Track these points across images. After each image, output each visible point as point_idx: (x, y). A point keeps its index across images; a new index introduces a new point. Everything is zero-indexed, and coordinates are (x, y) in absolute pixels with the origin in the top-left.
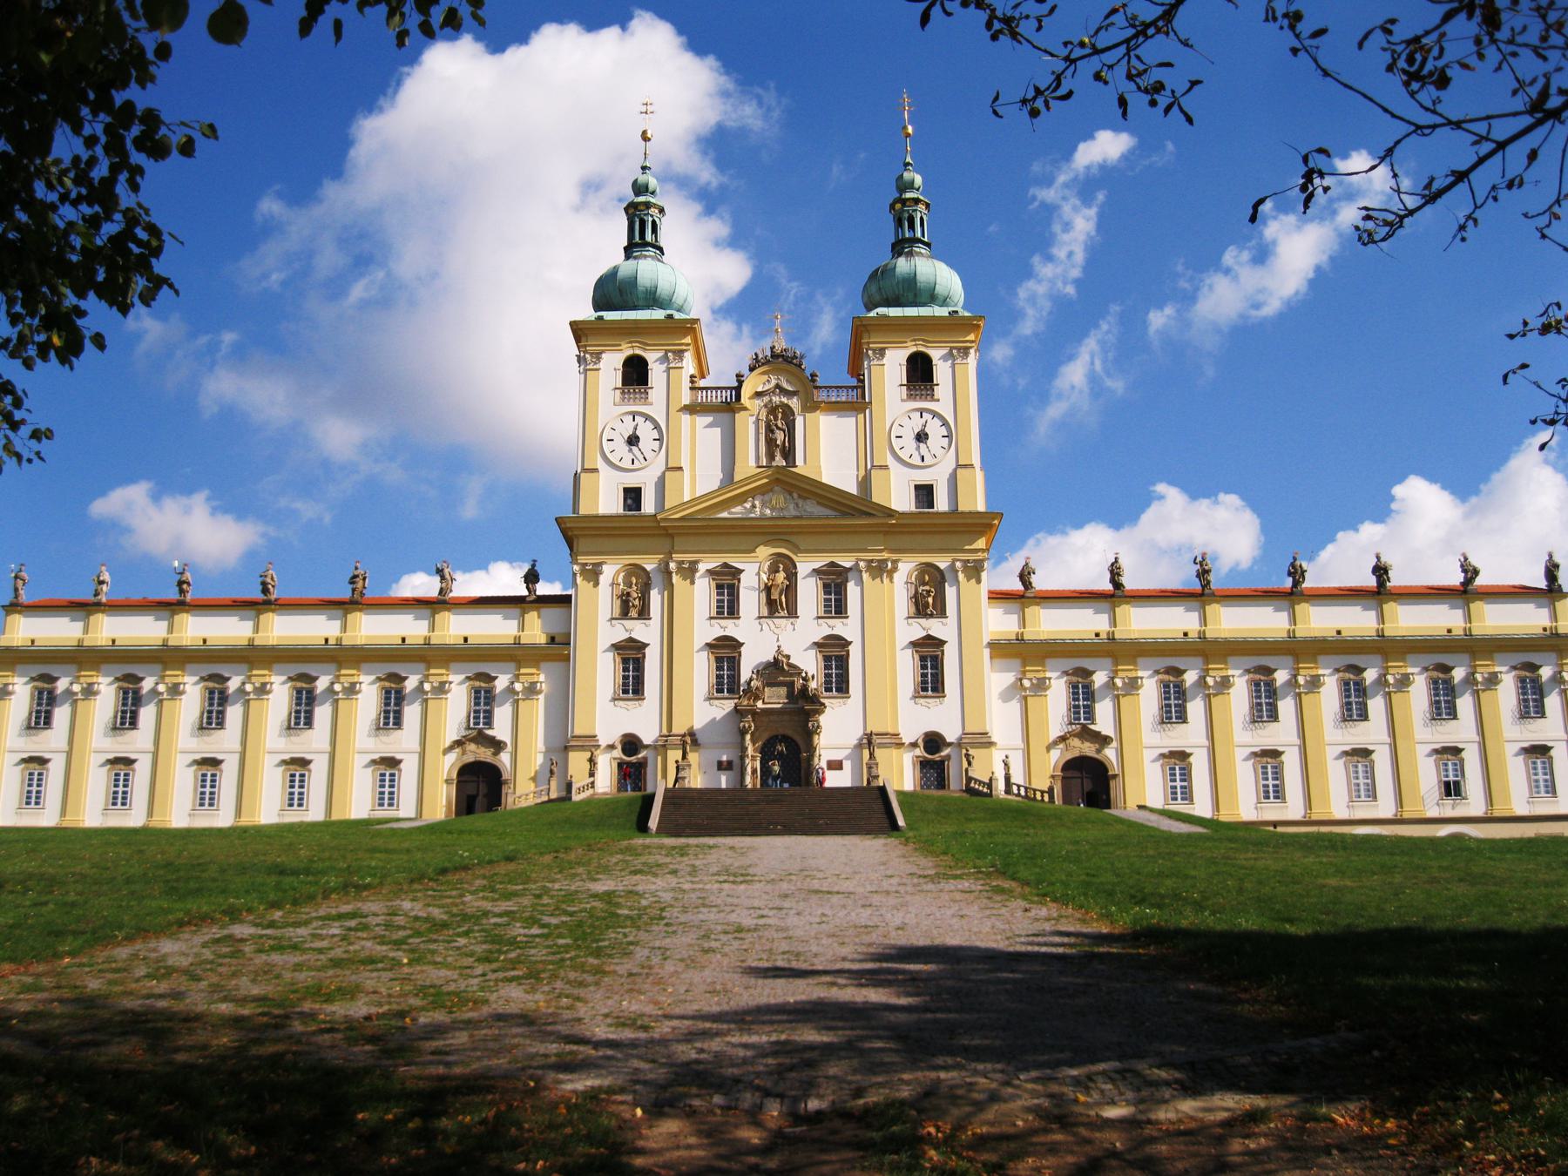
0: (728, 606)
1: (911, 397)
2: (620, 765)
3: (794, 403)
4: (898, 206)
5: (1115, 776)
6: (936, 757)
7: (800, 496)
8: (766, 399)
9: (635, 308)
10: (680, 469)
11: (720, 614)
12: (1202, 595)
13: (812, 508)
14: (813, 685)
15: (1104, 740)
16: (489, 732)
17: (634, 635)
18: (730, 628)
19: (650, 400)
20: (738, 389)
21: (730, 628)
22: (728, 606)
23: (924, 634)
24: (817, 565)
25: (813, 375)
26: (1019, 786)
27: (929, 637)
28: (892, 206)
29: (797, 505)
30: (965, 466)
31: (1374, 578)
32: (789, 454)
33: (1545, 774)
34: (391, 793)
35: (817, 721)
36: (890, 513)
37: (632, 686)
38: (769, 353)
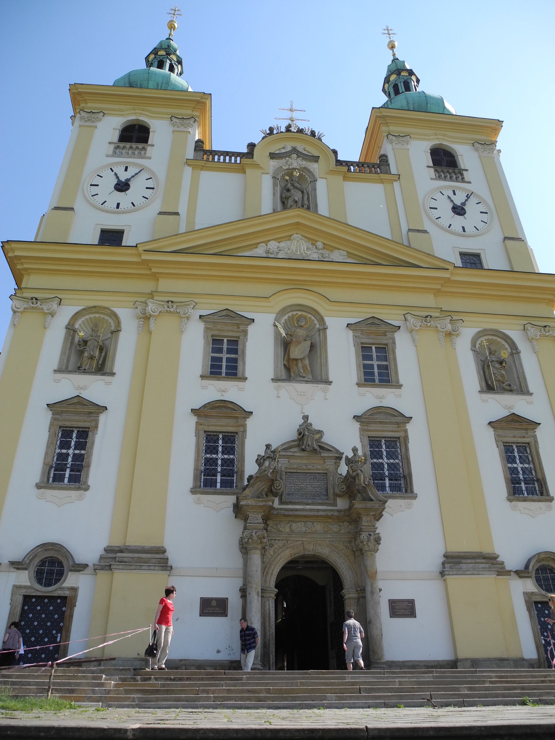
2: (27, 598)
3: (314, 167)
8: (282, 162)
10: (177, 214)
17: (86, 395)
19: (147, 155)
23: (505, 413)
24: (353, 321)
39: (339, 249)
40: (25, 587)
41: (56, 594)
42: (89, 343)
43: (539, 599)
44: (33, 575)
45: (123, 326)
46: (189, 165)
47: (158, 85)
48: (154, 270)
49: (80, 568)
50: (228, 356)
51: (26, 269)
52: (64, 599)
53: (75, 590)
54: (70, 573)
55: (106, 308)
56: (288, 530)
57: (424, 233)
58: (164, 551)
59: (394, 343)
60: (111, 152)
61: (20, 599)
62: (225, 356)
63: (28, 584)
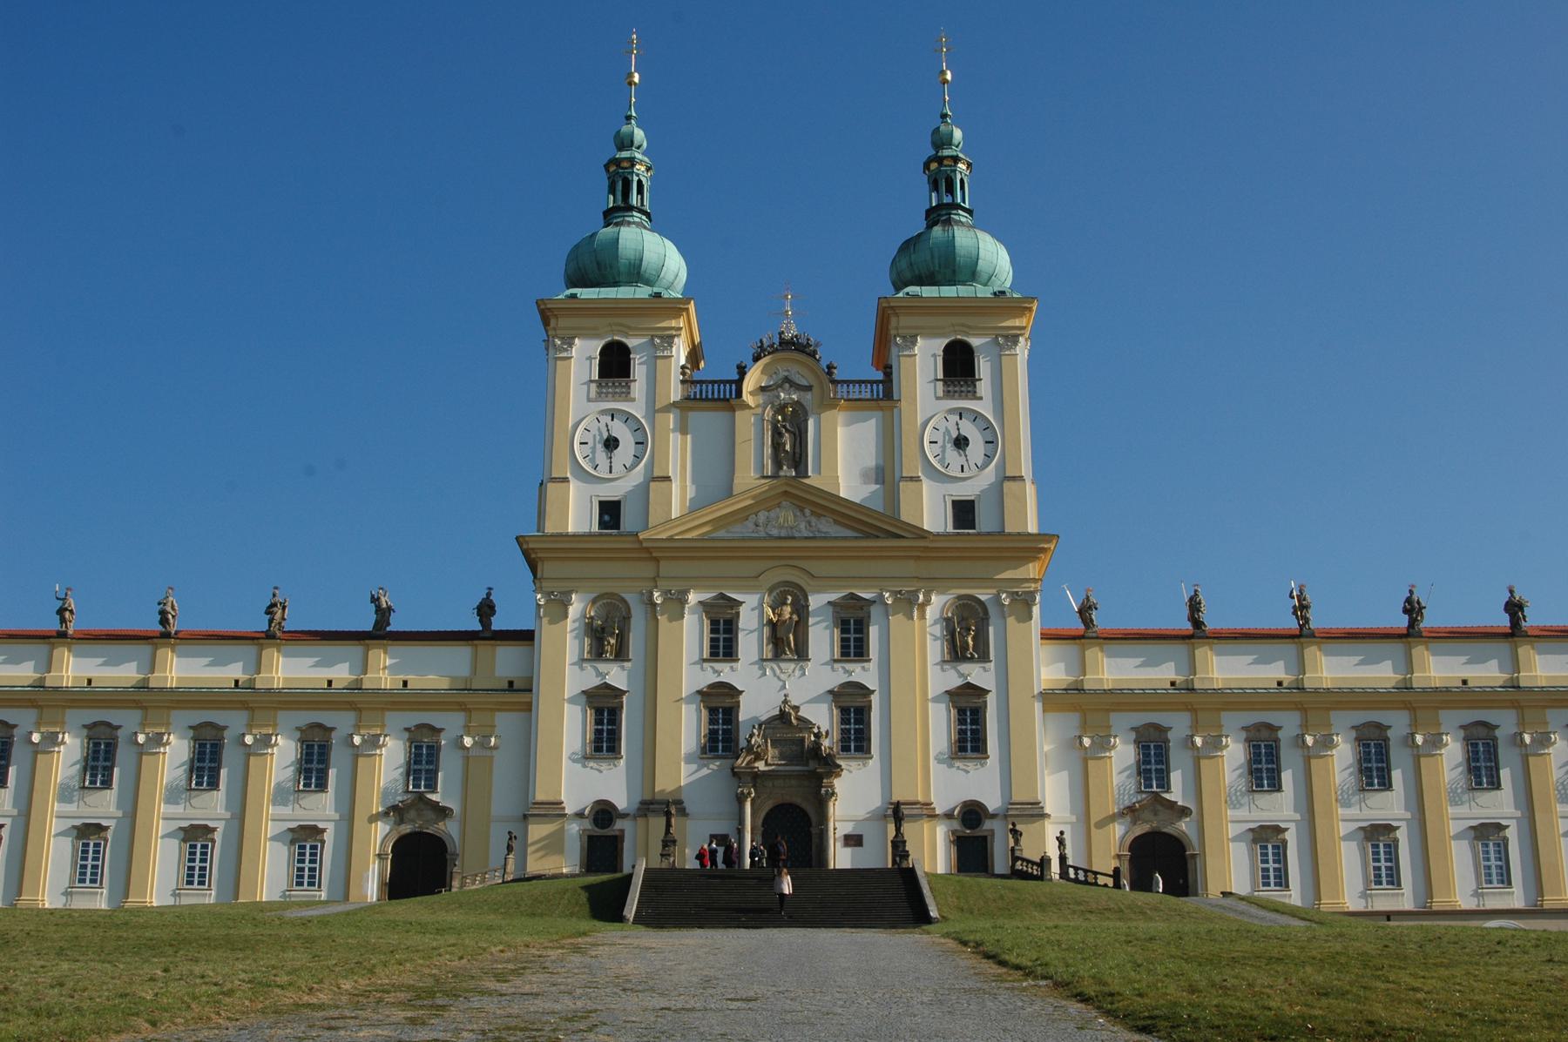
0: (723, 644)
1: (948, 395)
2: (590, 838)
3: (807, 398)
4: (934, 166)
5: (1194, 856)
6: (978, 832)
7: (813, 513)
9: (616, 284)
10: (668, 479)
11: (714, 654)
12: (1300, 636)
13: (827, 527)
14: (826, 743)
15: (1184, 812)
16: (434, 797)
17: (609, 680)
18: (726, 673)
19: (632, 395)
20: (739, 383)
21: (726, 673)
22: (723, 644)
25: (830, 367)
26: (1076, 869)
27: (969, 686)
28: (927, 166)
29: (809, 523)
30: (1014, 478)
31: (1506, 617)
32: (798, 460)
33: (1500, 860)
34: (203, 869)
35: (832, 787)
36: (922, 534)
37: (604, 742)
38: (777, 341)
39: (825, 516)
40: (588, 830)
41: (609, 834)
42: (606, 630)
43: (961, 834)
44: (592, 821)
45: (633, 611)
46: (677, 407)
47: (630, 263)
48: (654, 555)
49: (624, 816)
50: (725, 636)
51: (540, 558)
52: (615, 837)
53: (622, 831)
54: (618, 820)
55: (616, 594)
56: (771, 785)
57: (916, 481)
58: (683, 803)
59: (869, 617)
60: (593, 394)
61: (586, 837)
62: (722, 636)
63: (590, 828)
